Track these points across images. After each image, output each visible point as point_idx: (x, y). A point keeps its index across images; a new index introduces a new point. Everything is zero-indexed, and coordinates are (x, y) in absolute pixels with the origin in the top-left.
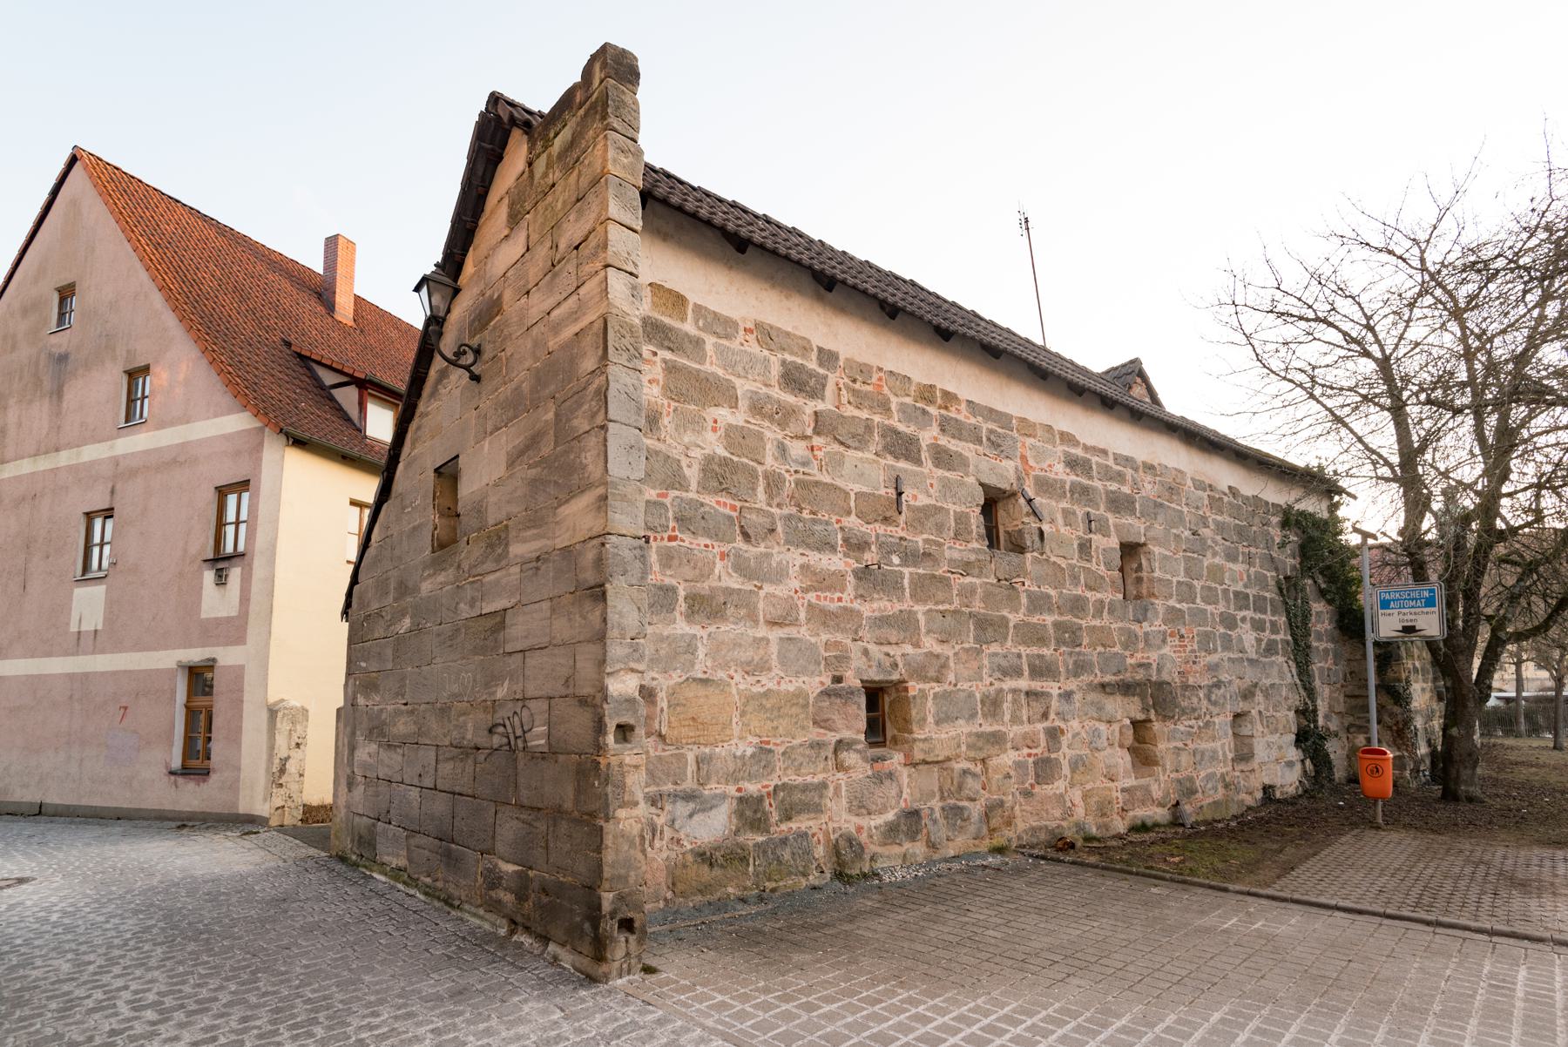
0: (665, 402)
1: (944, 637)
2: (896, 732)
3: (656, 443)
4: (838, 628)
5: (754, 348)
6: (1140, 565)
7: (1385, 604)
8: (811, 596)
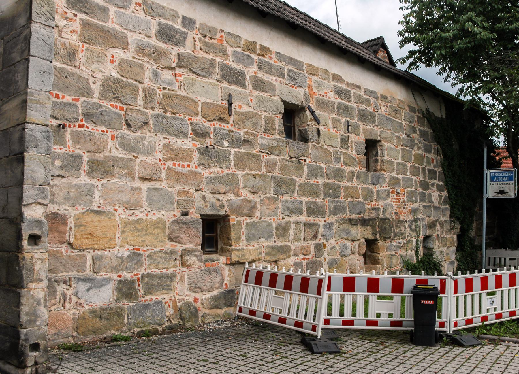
0: (81, 44)
1: (255, 190)
2: (223, 245)
3: (74, 68)
4: (186, 183)
5: (141, 15)
6: (377, 152)
7: (492, 179)
8: (170, 164)
